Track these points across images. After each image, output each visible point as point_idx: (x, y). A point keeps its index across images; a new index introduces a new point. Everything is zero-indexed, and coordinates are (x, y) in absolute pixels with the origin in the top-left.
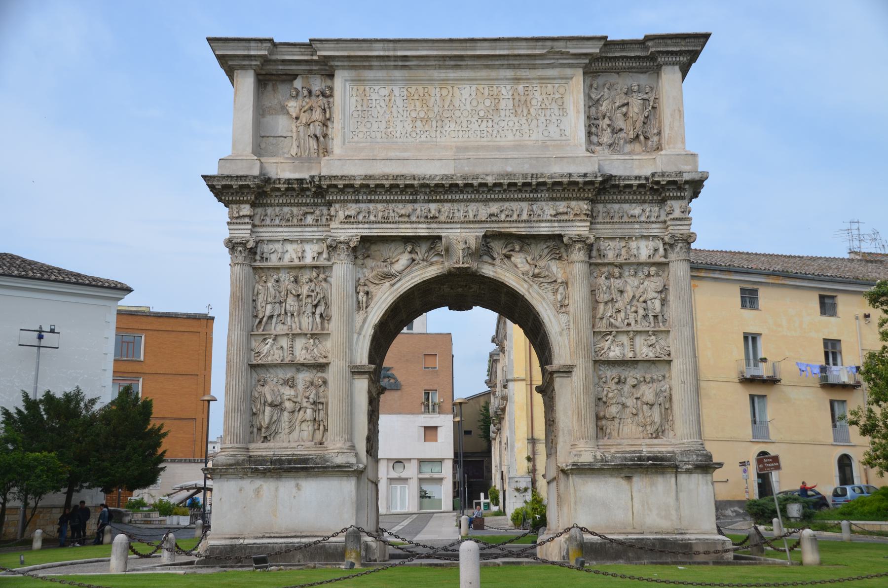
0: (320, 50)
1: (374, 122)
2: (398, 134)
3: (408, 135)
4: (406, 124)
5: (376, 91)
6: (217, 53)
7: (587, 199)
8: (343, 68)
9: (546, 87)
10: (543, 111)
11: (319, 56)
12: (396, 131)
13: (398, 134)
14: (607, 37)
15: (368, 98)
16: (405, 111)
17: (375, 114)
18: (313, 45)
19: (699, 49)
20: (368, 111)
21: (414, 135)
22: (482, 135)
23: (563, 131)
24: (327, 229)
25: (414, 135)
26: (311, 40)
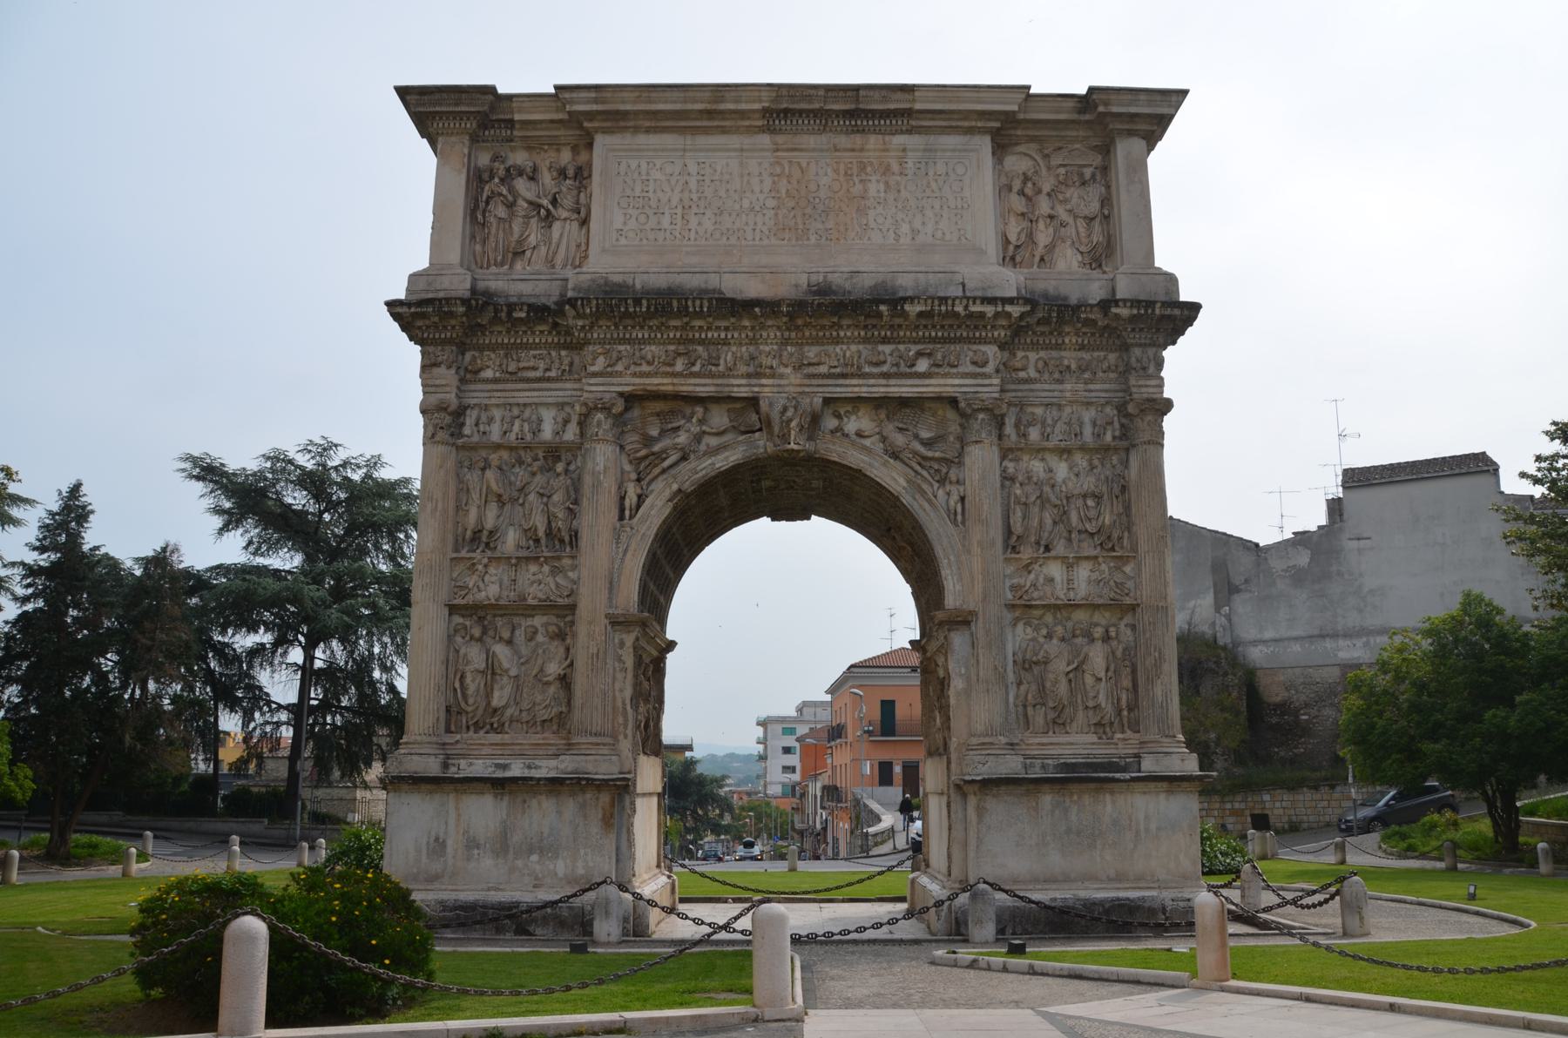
0: (569, 103)
2: (693, 232)
3: (708, 235)
5: (658, 166)
6: (413, 110)
7: (994, 341)
8: (605, 131)
9: (935, 163)
10: (930, 200)
11: (569, 112)
12: (690, 230)
13: (693, 232)
14: (1028, 87)
15: (644, 177)
17: (653, 203)
18: (560, 96)
19: (1173, 112)
20: (644, 197)
21: (717, 235)
23: (962, 232)
24: (577, 386)
25: (717, 235)
26: (557, 87)
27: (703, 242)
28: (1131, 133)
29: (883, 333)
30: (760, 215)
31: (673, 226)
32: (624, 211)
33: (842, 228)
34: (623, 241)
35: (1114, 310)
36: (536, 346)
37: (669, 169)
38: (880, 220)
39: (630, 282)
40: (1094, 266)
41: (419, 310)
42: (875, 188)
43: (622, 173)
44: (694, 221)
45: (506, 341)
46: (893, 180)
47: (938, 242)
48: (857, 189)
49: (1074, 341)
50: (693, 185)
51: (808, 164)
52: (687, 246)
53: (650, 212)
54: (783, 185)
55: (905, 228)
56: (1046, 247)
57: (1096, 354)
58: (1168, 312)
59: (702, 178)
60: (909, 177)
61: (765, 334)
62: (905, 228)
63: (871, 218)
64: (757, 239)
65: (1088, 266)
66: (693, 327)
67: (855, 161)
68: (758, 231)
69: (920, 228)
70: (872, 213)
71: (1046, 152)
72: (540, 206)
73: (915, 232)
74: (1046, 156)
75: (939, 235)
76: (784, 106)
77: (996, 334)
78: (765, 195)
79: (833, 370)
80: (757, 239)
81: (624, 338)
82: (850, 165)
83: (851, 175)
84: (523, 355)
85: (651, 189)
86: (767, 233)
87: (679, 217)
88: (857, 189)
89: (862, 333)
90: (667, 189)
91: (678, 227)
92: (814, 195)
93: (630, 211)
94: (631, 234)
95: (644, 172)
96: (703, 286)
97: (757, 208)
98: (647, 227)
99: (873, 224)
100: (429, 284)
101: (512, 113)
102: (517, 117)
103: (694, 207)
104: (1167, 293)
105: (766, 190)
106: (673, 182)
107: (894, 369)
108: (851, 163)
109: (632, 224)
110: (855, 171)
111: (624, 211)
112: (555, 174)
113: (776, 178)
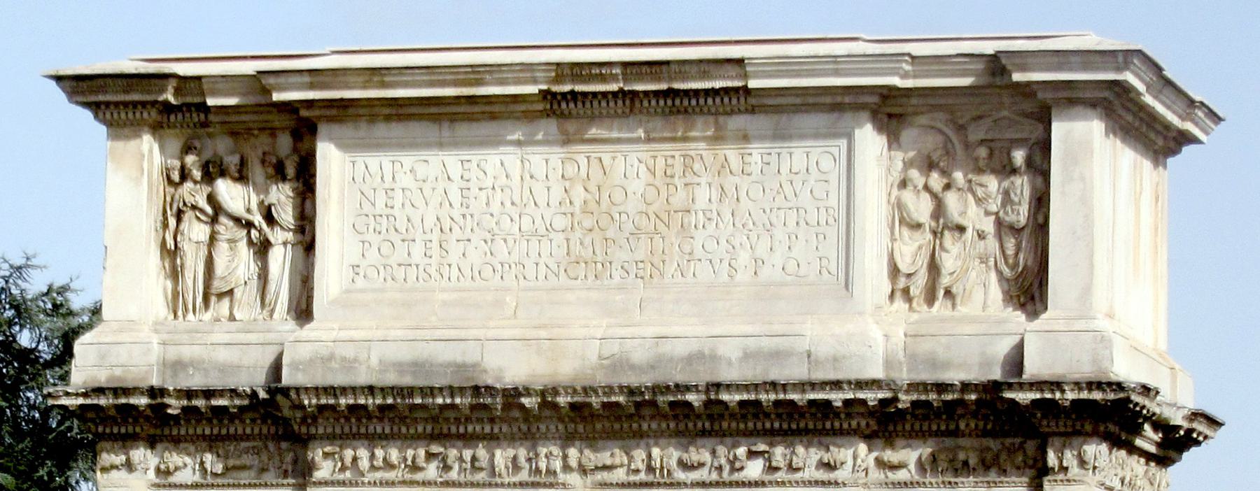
1: (398, 243)
4: (470, 248)
15: (387, 186)
16: (469, 217)
17: (402, 225)
21: (488, 272)
22: (641, 273)
27: (467, 283)
28: (1072, 102)
29: (700, 425)
30: (545, 241)
31: (427, 260)
32: (361, 237)
33: (656, 261)
34: (360, 283)
35: (1009, 395)
36: (246, 438)
37: (422, 170)
38: (710, 245)
39: (363, 356)
40: (1022, 299)
41: (89, 401)
42: (703, 195)
43: (359, 179)
44: (455, 250)
45: (207, 432)
46: (730, 182)
47: (789, 278)
48: (679, 198)
49: (973, 425)
50: (455, 197)
51: (614, 158)
52: (443, 290)
53: (396, 239)
54: (579, 194)
55: (744, 257)
56: (952, 274)
57: (1008, 441)
58: (1084, 395)
59: (464, 184)
60: (753, 178)
61: (543, 427)
62: (744, 257)
63: (698, 244)
64: (542, 277)
65: (1015, 300)
66: (447, 420)
67: (677, 154)
68: (542, 268)
69: (765, 257)
70: (700, 236)
71: (961, 122)
72: (249, 225)
73: (758, 262)
74: (961, 128)
75: (791, 266)
76: (566, 88)
77: (854, 423)
78: (553, 210)
79: (633, 478)
80: (542, 277)
81: (359, 434)
82: (670, 161)
83: (672, 177)
84: (232, 448)
85: (398, 203)
86: (554, 267)
87: (435, 244)
88: (679, 198)
89: (672, 425)
90: (419, 202)
91: (433, 261)
92: (621, 208)
93: (371, 236)
94: (372, 273)
95: (388, 178)
96: (459, 359)
97: (542, 231)
98: (393, 261)
99: (699, 252)
100: (103, 357)
101: (203, 94)
102: (211, 102)
103: (456, 228)
104: (1094, 361)
105: (554, 202)
106: (427, 192)
107: (714, 476)
108: (673, 157)
109: (373, 255)
110: (678, 169)
111: (361, 237)
112: (271, 171)
113: (567, 184)
